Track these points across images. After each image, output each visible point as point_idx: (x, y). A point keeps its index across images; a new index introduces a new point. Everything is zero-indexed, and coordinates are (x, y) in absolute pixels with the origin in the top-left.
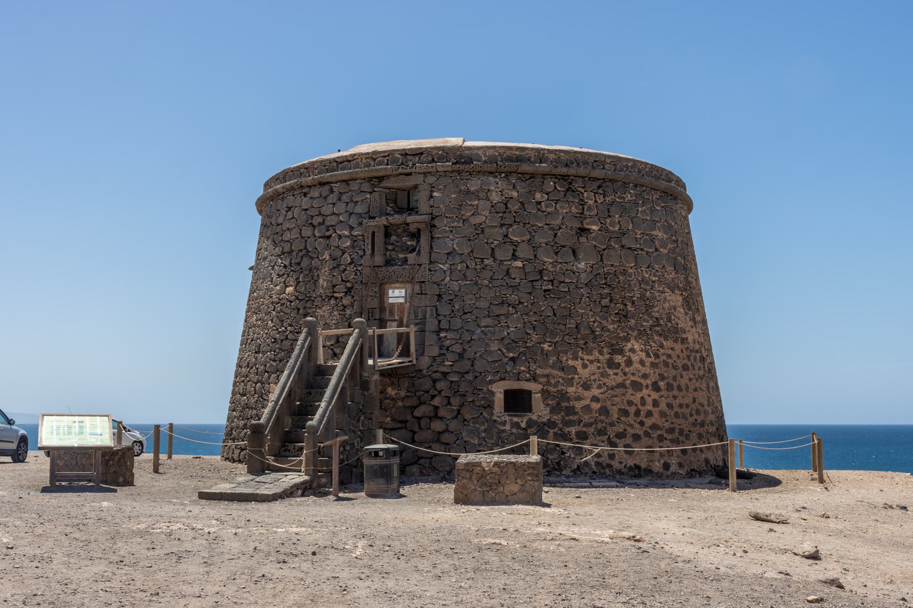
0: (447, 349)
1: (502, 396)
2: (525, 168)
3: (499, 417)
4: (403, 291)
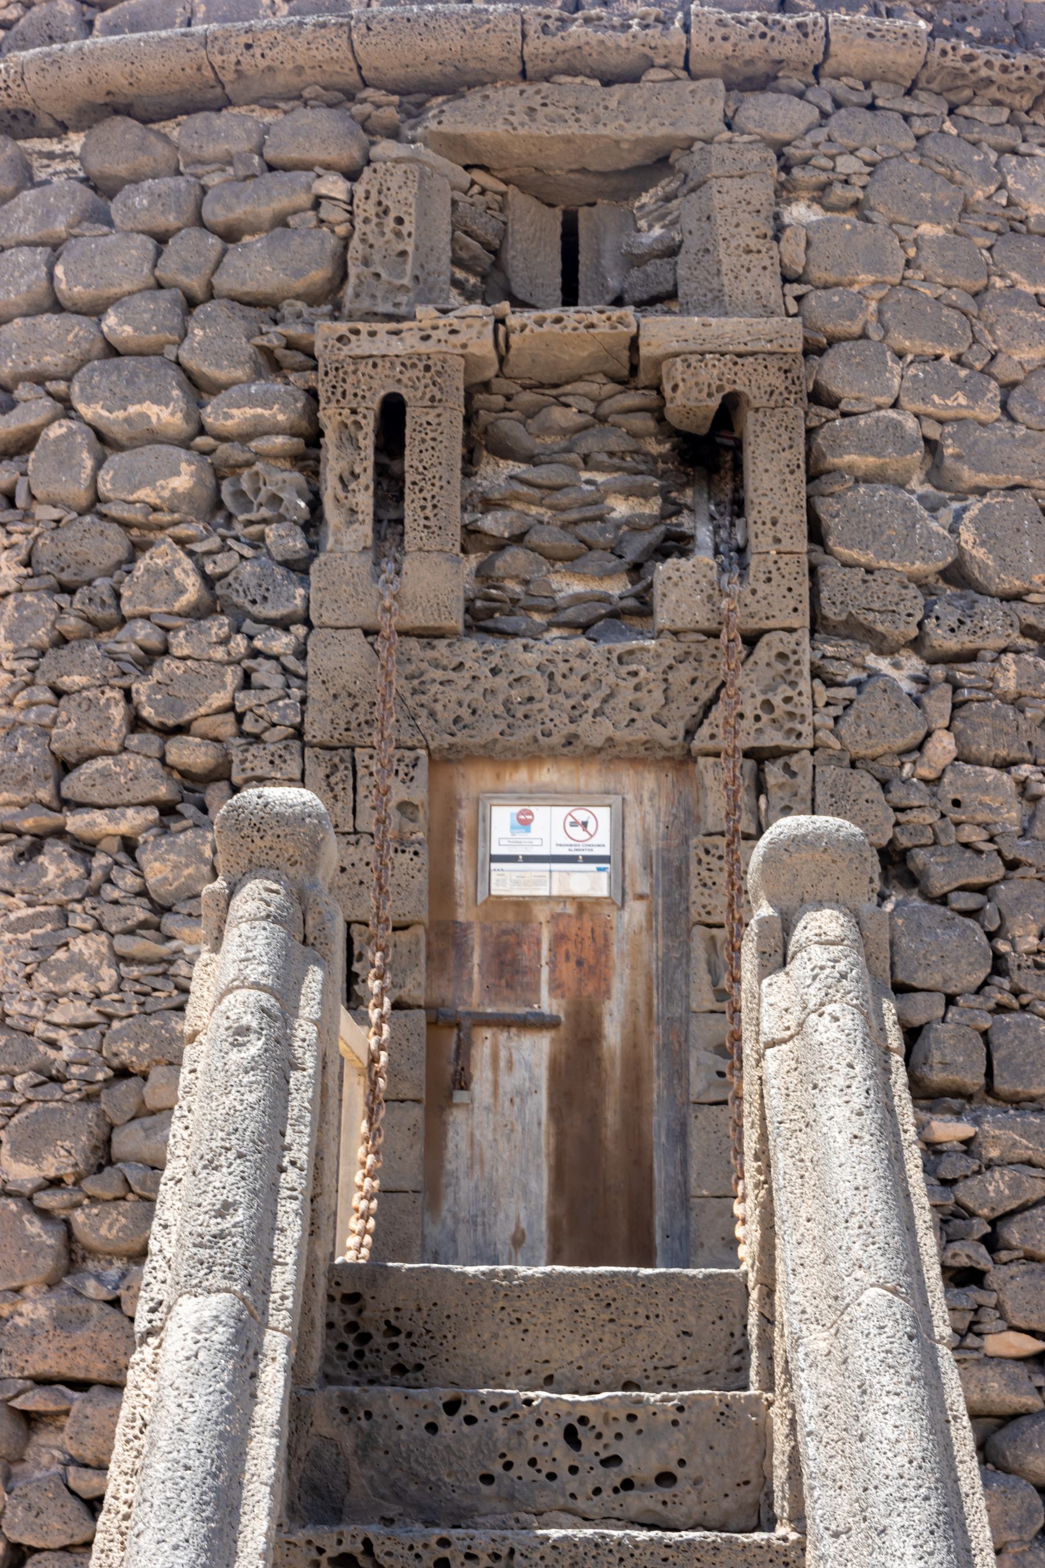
0: (992, 1243)
4: (602, 817)
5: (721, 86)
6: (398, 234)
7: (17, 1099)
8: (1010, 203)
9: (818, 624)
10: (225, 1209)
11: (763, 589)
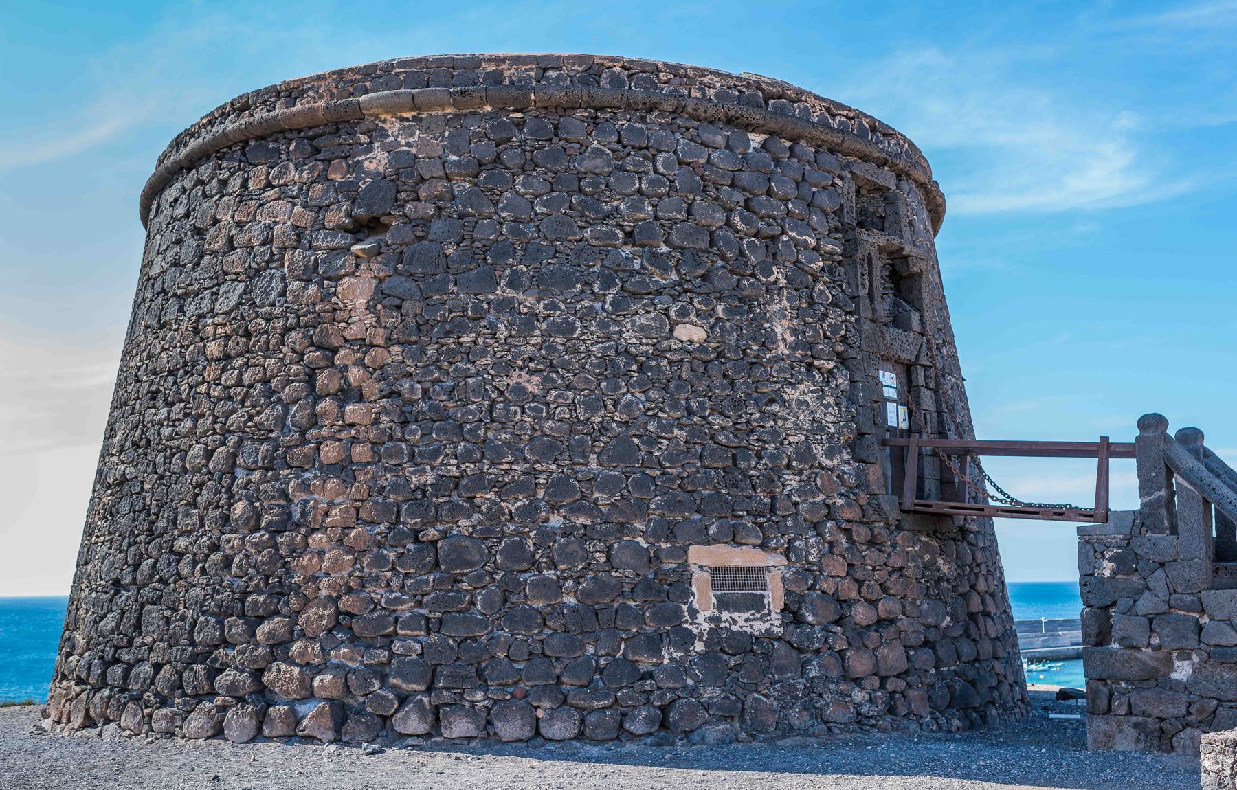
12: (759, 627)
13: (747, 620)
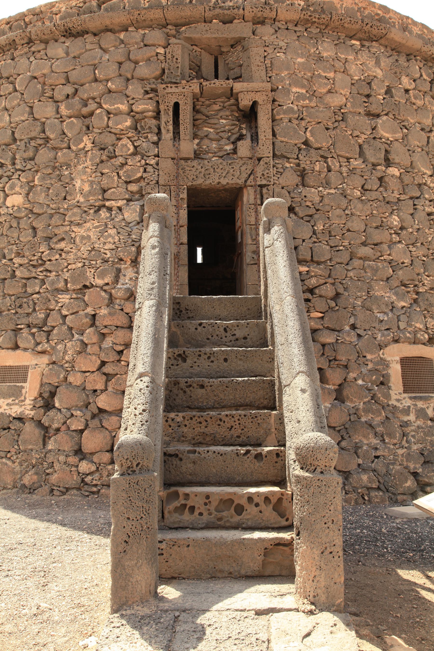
1: (398, 367)
2: (396, 35)
3: (398, 400)
5: (251, 23)
6: (177, 62)
7: (98, 266)
8: (319, 53)
9: (274, 155)
10: (153, 283)
11: (262, 147)
12: (15, 411)
13: (8, 404)
